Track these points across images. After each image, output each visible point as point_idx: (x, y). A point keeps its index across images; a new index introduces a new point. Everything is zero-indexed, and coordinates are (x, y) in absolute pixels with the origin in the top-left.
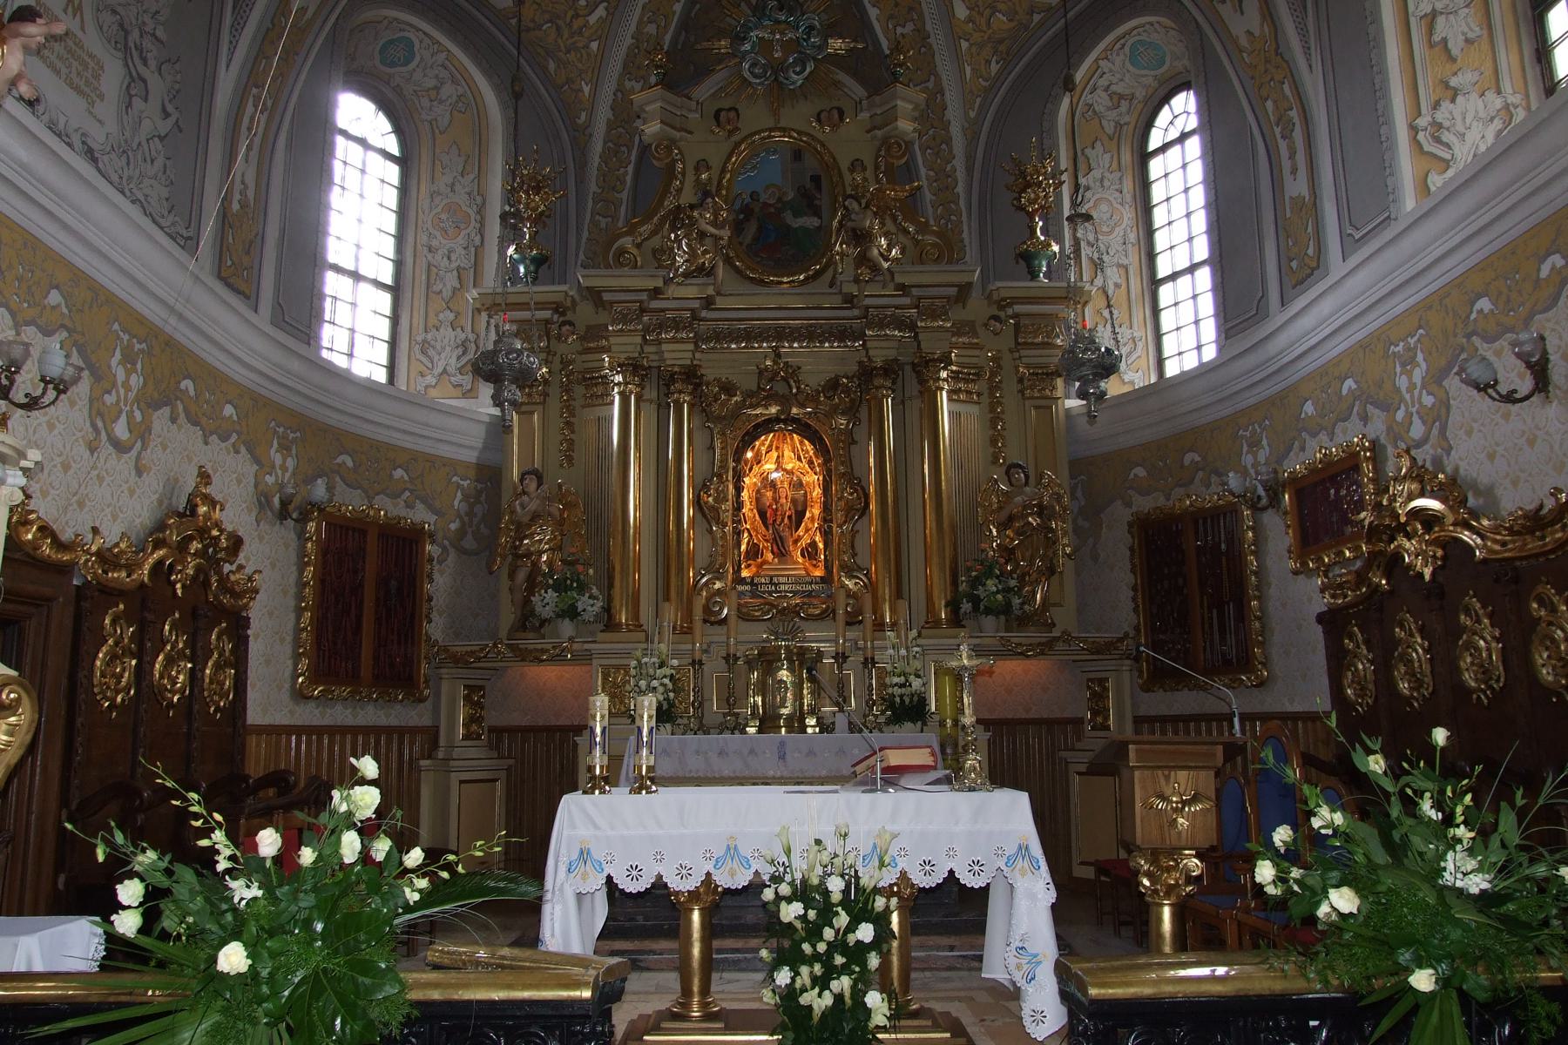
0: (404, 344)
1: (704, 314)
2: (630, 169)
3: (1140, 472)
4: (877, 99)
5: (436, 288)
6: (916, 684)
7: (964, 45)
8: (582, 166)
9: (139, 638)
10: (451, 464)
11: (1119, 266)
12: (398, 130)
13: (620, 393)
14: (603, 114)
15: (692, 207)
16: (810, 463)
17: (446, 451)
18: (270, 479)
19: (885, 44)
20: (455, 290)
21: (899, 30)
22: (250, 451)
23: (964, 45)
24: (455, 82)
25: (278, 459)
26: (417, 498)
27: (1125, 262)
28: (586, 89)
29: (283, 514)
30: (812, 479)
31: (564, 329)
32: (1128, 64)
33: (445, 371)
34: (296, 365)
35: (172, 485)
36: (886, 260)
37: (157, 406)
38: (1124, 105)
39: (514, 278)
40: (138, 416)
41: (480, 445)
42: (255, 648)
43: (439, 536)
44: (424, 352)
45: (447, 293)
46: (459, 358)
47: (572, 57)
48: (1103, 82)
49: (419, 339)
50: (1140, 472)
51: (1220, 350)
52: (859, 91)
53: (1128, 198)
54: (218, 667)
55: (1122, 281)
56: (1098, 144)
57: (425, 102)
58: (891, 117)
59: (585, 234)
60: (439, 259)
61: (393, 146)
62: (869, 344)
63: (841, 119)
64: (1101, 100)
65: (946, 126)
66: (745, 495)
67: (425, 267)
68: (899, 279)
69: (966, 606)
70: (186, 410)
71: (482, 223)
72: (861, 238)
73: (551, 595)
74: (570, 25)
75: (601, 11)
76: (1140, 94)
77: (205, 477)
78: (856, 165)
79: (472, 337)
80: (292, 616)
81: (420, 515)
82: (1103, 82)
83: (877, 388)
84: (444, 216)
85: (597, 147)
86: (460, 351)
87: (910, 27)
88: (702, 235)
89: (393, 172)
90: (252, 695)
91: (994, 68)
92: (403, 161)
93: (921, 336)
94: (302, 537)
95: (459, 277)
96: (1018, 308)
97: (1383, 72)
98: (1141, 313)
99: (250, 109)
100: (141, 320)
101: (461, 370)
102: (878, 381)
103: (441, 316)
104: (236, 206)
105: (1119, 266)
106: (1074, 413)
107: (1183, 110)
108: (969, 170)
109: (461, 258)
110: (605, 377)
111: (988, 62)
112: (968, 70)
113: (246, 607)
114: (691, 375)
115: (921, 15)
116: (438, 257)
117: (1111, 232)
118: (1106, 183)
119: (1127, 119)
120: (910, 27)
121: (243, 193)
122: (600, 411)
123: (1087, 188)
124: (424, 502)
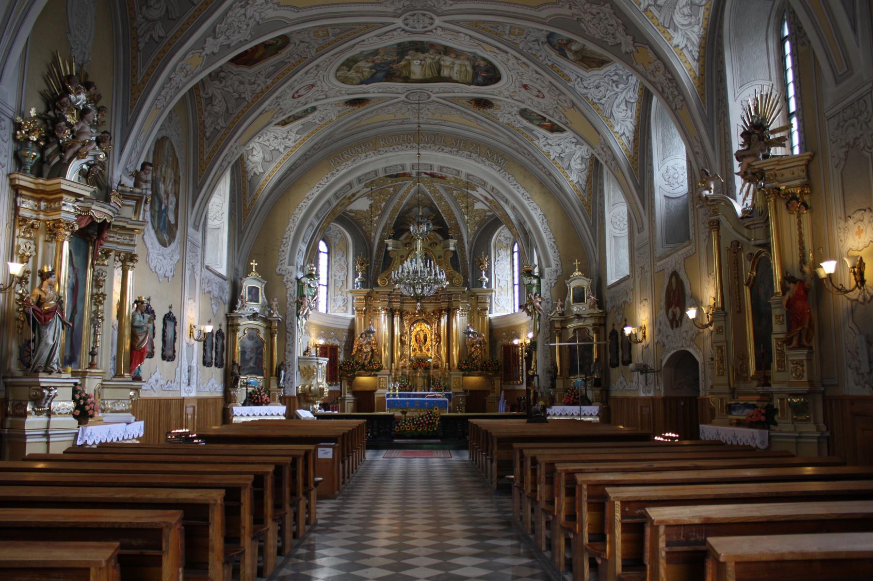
0: (329, 299)
8: (371, 252)
10: (342, 330)
14: (377, 241)
17: (341, 327)
28: (373, 234)
45: (340, 286)
52: (441, 238)
58: (448, 246)
60: (337, 278)
64: (502, 238)
65: (464, 244)
75: (377, 218)
78: (440, 257)
81: (337, 343)
91: (476, 228)
108: (470, 254)
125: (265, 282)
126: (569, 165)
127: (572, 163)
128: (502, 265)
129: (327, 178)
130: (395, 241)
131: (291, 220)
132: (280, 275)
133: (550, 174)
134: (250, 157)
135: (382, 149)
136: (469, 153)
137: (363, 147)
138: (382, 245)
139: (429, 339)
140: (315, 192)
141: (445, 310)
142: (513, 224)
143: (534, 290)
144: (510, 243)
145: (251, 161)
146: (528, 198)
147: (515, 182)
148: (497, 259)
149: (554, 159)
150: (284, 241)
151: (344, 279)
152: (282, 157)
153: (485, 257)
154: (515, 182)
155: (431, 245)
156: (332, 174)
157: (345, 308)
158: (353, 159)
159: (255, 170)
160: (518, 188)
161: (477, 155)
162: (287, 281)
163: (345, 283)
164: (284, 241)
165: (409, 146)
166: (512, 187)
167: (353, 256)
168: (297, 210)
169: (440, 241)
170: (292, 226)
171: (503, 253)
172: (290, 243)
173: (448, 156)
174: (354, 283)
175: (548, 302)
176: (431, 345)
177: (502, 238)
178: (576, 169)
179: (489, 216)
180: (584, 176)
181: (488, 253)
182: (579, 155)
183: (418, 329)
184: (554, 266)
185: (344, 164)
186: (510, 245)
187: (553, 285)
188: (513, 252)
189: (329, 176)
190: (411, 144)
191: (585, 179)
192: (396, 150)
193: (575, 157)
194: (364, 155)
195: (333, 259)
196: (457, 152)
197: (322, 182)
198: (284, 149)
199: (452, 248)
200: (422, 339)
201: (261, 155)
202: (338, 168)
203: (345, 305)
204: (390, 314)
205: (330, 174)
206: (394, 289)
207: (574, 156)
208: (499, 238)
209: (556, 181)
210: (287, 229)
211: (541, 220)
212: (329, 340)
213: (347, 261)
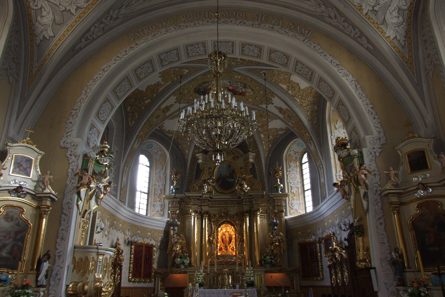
0: (149, 205)
1: (210, 200)
2: (196, 167)
3: (300, 233)
4: (245, 155)
5: (156, 193)
6: (252, 278)
7: (264, 142)
9: (114, 271)
11: (297, 187)
12: (149, 161)
13: (194, 217)
15: (208, 179)
16: (233, 230)
18: (126, 237)
19: (247, 142)
20: (160, 194)
21: (250, 140)
22: (123, 232)
23: (264, 142)
24: (161, 151)
25: (127, 233)
26: (152, 238)
27: (298, 186)
28: (187, 152)
29: (128, 244)
30: (233, 233)
31: (182, 203)
32: (297, 146)
33: (158, 211)
34: (131, 215)
35: (113, 242)
36: (246, 190)
37: (110, 227)
38: (297, 154)
39: (173, 193)
40: (108, 229)
41: (165, 227)
42: (123, 271)
43: (156, 246)
44: (153, 207)
45: (158, 194)
46: (161, 208)
47: (184, 145)
48: (292, 149)
49: (153, 204)
50: (300, 233)
51: (313, 209)
52: (242, 153)
53: (299, 173)
54: (118, 275)
55: (297, 191)
56: (292, 162)
57: (155, 155)
58: (248, 158)
59: (186, 181)
61: (148, 164)
62: (244, 206)
63: (238, 159)
64: (292, 153)
65: (260, 158)
66: (219, 237)
67: (154, 189)
68: (249, 194)
69: (263, 262)
70: (115, 227)
71: (166, 180)
72: (242, 185)
73: (179, 259)
74: (184, 139)
76: (300, 152)
77: (118, 239)
78: (241, 168)
79: (163, 204)
80: (129, 264)
81: (153, 242)
82: (292, 149)
83: (245, 215)
84: (158, 178)
85: (189, 163)
86: (161, 206)
87: (252, 140)
88: (210, 185)
89: (148, 169)
90: (122, 281)
91: (270, 146)
92: (150, 167)
93: (254, 205)
94: (131, 248)
95: (161, 191)
96: (275, 198)
97: (331, 164)
98: (301, 197)
99: (126, 167)
100: (110, 212)
101: (161, 211)
102: (245, 214)
103: (157, 199)
104: (123, 186)
105: (297, 187)
106: (287, 220)
107: (305, 158)
108: (266, 167)
109: (162, 188)
110: (190, 213)
111: (269, 145)
112: (265, 147)
113: (122, 263)
114: (207, 213)
115: (254, 137)
116: (157, 187)
117: (295, 180)
118: (294, 170)
119: (298, 156)
120: (252, 140)
121: (124, 183)
122: (189, 220)
123: (290, 171)
124: (153, 239)
125: (42, 153)
126: (384, 19)
127: (388, 17)
128: (293, 175)
129: (126, 51)
130: (205, 155)
131: (84, 92)
132: (64, 148)
133: (362, 34)
134: (39, 18)
135: (183, 24)
136: (272, 26)
137: (164, 24)
138: (194, 159)
139: (233, 240)
140: (113, 65)
141: (247, 212)
142: (306, 128)
143: (356, 161)
144: (299, 156)
145: (40, 24)
146: (337, 65)
147: (321, 51)
148: (288, 170)
149: (366, 14)
150: (74, 112)
151: (162, 188)
152: (74, 19)
153: (279, 167)
154: (321, 51)
155: (233, 158)
156: (131, 47)
157: (162, 213)
158: (153, 34)
159: (44, 33)
160: (325, 55)
161: (280, 27)
162: (71, 155)
163: (163, 191)
164: (74, 112)
165: (210, 21)
166: (318, 55)
167: (171, 168)
168: (91, 82)
169: (242, 155)
170: (84, 97)
171: (292, 164)
172: (80, 115)
173: (249, 29)
174: (170, 191)
175: (375, 175)
176: (236, 246)
177: (292, 153)
178: (393, 24)
179: (281, 135)
180: (402, 30)
181: (281, 164)
182: (395, 5)
183: (224, 230)
184: (375, 134)
185: (144, 38)
186: (298, 159)
187: (378, 154)
188: (301, 164)
189: (127, 49)
190: (212, 20)
191: (404, 33)
192: (197, 24)
193: (391, 8)
194: (164, 30)
195: (154, 172)
196: (259, 25)
197: (120, 55)
198: (76, 10)
199: (251, 160)
200: (228, 239)
201: (51, 16)
202: (138, 42)
203: (163, 210)
204: (200, 217)
205: (128, 48)
206: (203, 194)
207: (390, 8)
208: (289, 152)
209: (369, 41)
210: (78, 100)
211: (354, 85)
212: (145, 240)
213: (165, 173)
